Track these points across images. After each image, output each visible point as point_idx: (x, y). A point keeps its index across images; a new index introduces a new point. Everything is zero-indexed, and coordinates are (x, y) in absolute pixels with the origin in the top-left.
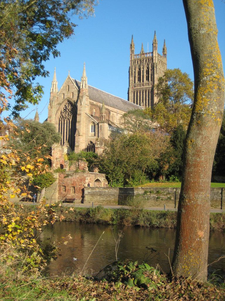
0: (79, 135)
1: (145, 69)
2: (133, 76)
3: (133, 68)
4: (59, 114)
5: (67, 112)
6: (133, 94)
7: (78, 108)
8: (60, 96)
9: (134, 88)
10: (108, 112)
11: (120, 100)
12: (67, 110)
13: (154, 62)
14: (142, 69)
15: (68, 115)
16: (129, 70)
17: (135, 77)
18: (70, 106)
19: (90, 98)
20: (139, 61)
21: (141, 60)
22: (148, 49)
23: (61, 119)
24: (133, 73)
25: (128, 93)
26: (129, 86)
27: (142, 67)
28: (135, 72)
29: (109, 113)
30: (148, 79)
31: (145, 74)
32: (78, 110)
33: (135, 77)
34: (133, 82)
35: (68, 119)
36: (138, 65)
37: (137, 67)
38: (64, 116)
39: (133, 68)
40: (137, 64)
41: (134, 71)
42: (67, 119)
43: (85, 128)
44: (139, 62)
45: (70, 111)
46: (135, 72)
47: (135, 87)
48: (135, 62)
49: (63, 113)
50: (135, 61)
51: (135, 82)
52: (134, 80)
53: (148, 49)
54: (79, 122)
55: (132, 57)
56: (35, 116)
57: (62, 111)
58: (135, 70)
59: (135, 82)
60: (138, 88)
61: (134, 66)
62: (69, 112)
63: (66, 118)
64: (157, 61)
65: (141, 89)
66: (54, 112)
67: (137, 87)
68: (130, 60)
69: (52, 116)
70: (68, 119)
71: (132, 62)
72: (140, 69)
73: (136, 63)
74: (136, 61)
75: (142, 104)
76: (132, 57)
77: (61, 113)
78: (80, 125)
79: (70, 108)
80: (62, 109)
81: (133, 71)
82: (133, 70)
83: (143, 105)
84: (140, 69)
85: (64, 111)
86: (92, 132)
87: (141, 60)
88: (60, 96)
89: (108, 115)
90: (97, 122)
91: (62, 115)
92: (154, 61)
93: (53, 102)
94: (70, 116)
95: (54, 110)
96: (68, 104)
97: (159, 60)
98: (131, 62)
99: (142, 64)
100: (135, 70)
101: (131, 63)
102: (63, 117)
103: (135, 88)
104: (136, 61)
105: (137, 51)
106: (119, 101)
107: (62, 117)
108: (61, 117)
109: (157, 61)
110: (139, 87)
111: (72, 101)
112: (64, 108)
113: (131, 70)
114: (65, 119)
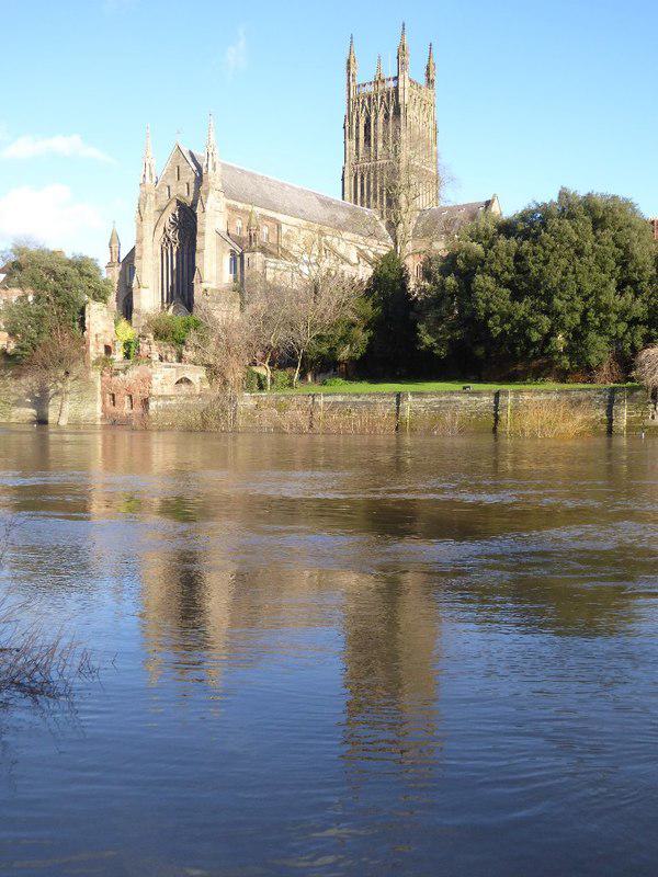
17: (357, 139)
20: (366, 100)
25: (343, 180)
27: (373, 115)
28: (357, 128)
29: (279, 227)
33: (357, 139)
38: (171, 237)
44: (366, 103)
54: (202, 250)
56: (111, 240)
58: (358, 121)
72: (368, 120)
84: (368, 120)
95: (149, 225)
105: (364, 74)
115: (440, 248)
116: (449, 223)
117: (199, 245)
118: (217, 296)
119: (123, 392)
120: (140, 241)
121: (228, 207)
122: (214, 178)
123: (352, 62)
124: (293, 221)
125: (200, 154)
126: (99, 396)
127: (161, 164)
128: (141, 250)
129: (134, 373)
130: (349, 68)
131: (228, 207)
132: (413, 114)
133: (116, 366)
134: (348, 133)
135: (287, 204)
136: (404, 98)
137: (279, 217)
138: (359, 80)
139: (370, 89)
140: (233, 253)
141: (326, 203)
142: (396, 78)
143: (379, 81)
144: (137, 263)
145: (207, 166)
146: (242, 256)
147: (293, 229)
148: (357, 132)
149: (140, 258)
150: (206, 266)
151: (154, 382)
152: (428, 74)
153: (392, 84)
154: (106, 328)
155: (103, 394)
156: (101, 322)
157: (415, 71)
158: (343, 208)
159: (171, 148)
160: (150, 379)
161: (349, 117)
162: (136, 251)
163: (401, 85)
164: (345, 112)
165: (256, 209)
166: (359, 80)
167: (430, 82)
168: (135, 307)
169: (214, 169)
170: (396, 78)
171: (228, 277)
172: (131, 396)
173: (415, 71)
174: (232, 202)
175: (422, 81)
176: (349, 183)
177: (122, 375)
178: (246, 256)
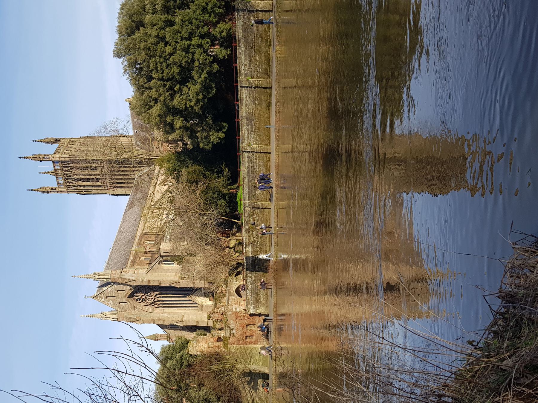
0: (179, 282)
1: (79, 172)
2: (91, 188)
3: (79, 188)
4: (149, 308)
5: (145, 298)
6: (118, 189)
7: (138, 284)
8: (123, 308)
9: (109, 187)
10: (146, 236)
11: (128, 213)
12: (144, 297)
13: (68, 160)
14: (80, 177)
15: (150, 296)
16: (83, 194)
17: (92, 186)
18: (137, 294)
19: (126, 264)
20: (67, 181)
21: (66, 177)
22: (49, 166)
23: (155, 305)
24: (86, 188)
26: (106, 194)
28: (85, 186)
29: (146, 234)
30: (95, 169)
31: (87, 172)
32: (142, 284)
33: (92, 186)
34: (100, 188)
35: (156, 296)
36: (74, 182)
37: (77, 183)
38: (151, 302)
39: (79, 188)
40: (72, 183)
41: (82, 188)
42: (155, 298)
43: (168, 274)
44: (69, 180)
45: (145, 294)
46: (85, 186)
47: (107, 186)
48: (69, 186)
49: (147, 302)
50: (68, 187)
51: (100, 186)
52: (97, 188)
53: (49, 166)
55: (62, 191)
56: (153, 339)
57: (144, 304)
58: (80, 186)
59: (100, 186)
60: (109, 181)
61: (75, 187)
62: (146, 295)
63: (155, 299)
64: (65, 156)
65: (110, 177)
66: (146, 315)
67: (108, 184)
68: (66, 194)
69: (152, 318)
70: (156, 296)
71: (69, 190)
73: (71, 184)
74: (68, 184)
75: (133, 177)
76: (62, 190)
77: (147, 305)
78: (163, 281)
79: (140, 295)
80: (141, 304)
81: (84, 188)
82: (81, 189)
83: (134, 175)
85: (144, 301)
86: (173, 264)
87: (66, 178)
88: (123, 308)
89: (148, 236)
90: (159, 257)
91: (150, 304)
92: (66, 160)
93: (131, 318)
94: (151, 293)
95: (144, 315)
96: (134, 296)
97: (65, 151)
98: (68, 191)
99: (72, 176)
100: (80, 186)
101: (70, 191)
102: (153, 303)
103: (108, 185)
104: (68, 184)
105: (51, 182)
106: (129, 214)
107: (153, 304)
108: (153, 306)
109: (65, 156)
110: (107, 180)
111: (130, 292)
112: (140, 301)
113: (82, 191)
114: (156, 300)
115: (158, 134)
116: (141, 127)
117: (156, 284)
118: (186, 273)
119: (245, 330)
120: (154, 321)
121: (132, 266)
122: (115, 275)
123: (44, 190)
124: (141, 225)
125: (98, 283)
126: (249, 346)
127: (107, 308)
128: (159, 320)
129: (233, 324)
130: (48, 192)
131: (132, 266)
132: (75, 152)
133: (228, 335)
134: (86, 192)
135: (131, 229)
136: (66, 157)
137: (139, 232)
138: (55, 185)
139: (60, 179)
140: (160, 262)
141: (131, 205)
142: (53, 162)
143: (55, 173)
144: (167, 323)
145: (106, 279)
146: (162, 257)
147: (146, 225)
148: (87, 186)
149: (164, 321)
150: (169, 279)
151: (238, 310)
152: (51, 143)
153: (57, 164)
154: (204, 341)
155: (246, 343)
156: (201, 344)
157: (50, 150)
158: (135, 195)
159: (94, 301)
160: (236, 313)
161: (79, 192)
162: (160, 323)
163: (58, 159)
164: (75, 195)
165: (134, 248)
166: (55, 185)
167: (57, 141)
168: (195, 324)
169: (108, 274)
170: (53, 162)
171: (175, 266)
172: (247, 326)
173: (50, 150)
174: (129, 263)
175: (56, 146)
176: (119, 191)
177: (234, 331)
178: (162, 254)
